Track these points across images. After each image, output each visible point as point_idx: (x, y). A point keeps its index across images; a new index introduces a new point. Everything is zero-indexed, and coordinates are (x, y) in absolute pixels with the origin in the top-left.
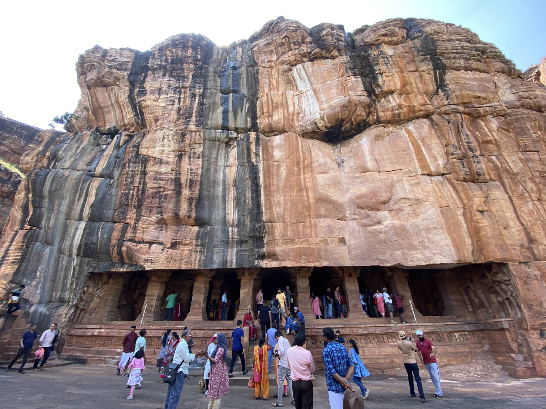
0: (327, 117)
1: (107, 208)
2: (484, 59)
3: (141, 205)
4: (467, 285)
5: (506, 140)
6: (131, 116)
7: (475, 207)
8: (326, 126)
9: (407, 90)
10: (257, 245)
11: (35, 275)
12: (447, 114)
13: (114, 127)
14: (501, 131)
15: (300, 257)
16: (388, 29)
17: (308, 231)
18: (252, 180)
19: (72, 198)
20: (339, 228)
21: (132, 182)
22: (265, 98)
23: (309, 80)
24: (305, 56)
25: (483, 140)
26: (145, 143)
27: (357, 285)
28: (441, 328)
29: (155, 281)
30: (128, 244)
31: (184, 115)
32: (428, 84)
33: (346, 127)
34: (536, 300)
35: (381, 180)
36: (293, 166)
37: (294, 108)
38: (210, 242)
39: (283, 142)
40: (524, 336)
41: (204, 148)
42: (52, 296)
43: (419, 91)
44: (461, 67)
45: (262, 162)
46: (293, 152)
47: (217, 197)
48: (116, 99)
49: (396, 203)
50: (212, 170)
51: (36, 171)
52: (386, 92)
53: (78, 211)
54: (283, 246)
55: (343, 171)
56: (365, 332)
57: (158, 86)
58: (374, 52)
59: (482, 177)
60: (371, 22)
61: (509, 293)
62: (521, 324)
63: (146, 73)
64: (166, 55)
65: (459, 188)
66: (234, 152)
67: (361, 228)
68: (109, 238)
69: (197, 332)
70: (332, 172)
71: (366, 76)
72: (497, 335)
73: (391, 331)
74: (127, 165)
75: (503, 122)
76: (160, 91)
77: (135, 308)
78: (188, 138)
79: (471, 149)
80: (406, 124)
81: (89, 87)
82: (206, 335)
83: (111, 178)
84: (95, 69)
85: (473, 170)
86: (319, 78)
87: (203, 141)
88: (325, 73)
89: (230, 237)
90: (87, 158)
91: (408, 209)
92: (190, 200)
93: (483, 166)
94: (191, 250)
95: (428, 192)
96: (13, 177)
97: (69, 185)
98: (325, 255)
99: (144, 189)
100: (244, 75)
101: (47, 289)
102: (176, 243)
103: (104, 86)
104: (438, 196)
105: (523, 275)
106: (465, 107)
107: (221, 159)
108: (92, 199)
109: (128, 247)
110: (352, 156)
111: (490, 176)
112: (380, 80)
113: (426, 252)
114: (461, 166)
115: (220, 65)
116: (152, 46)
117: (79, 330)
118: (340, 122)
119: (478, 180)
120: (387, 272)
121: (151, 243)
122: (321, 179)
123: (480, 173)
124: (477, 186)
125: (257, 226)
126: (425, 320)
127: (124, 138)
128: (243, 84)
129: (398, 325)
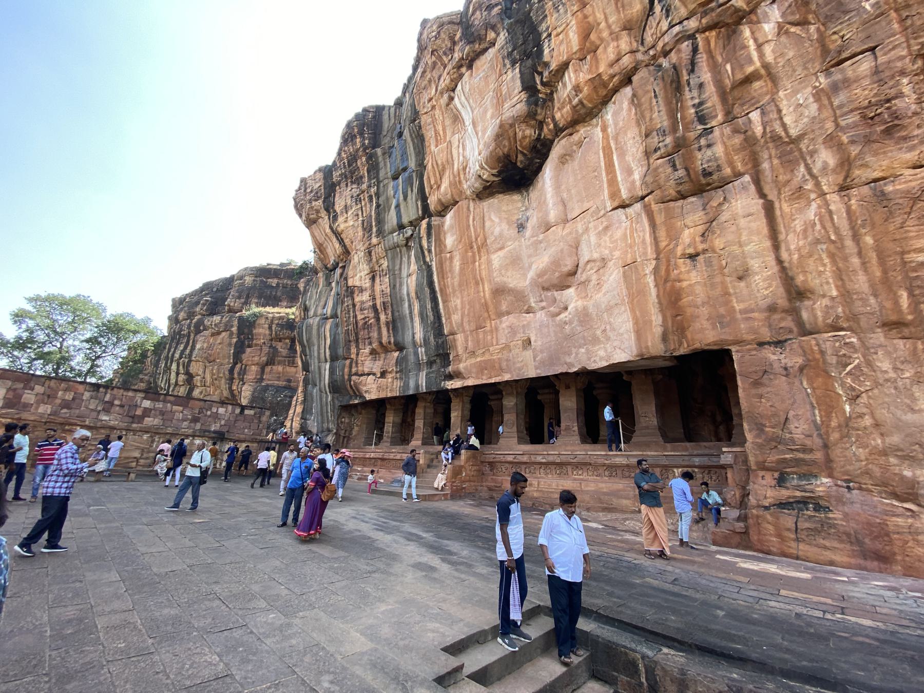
20: (524, 326)
22: (430, 164)
24: (461, 66)
30: (354, 378)
31: (367, 229)
33: (521, 162)
36: (466, 251)
50: (398, 285)
52: (557, 71)
56: (544, 461)
59: (715, 177)
65: (659, 219)
68: (343, 375)
76: (346, 208)
79: (702, 119)
85: (694, 169)
92: (387, 324)
106: (705, 13)
111: (733, 168)
112: (546, 51)
114: (670, 170)
119: (709, 184)
121: (368, 374)
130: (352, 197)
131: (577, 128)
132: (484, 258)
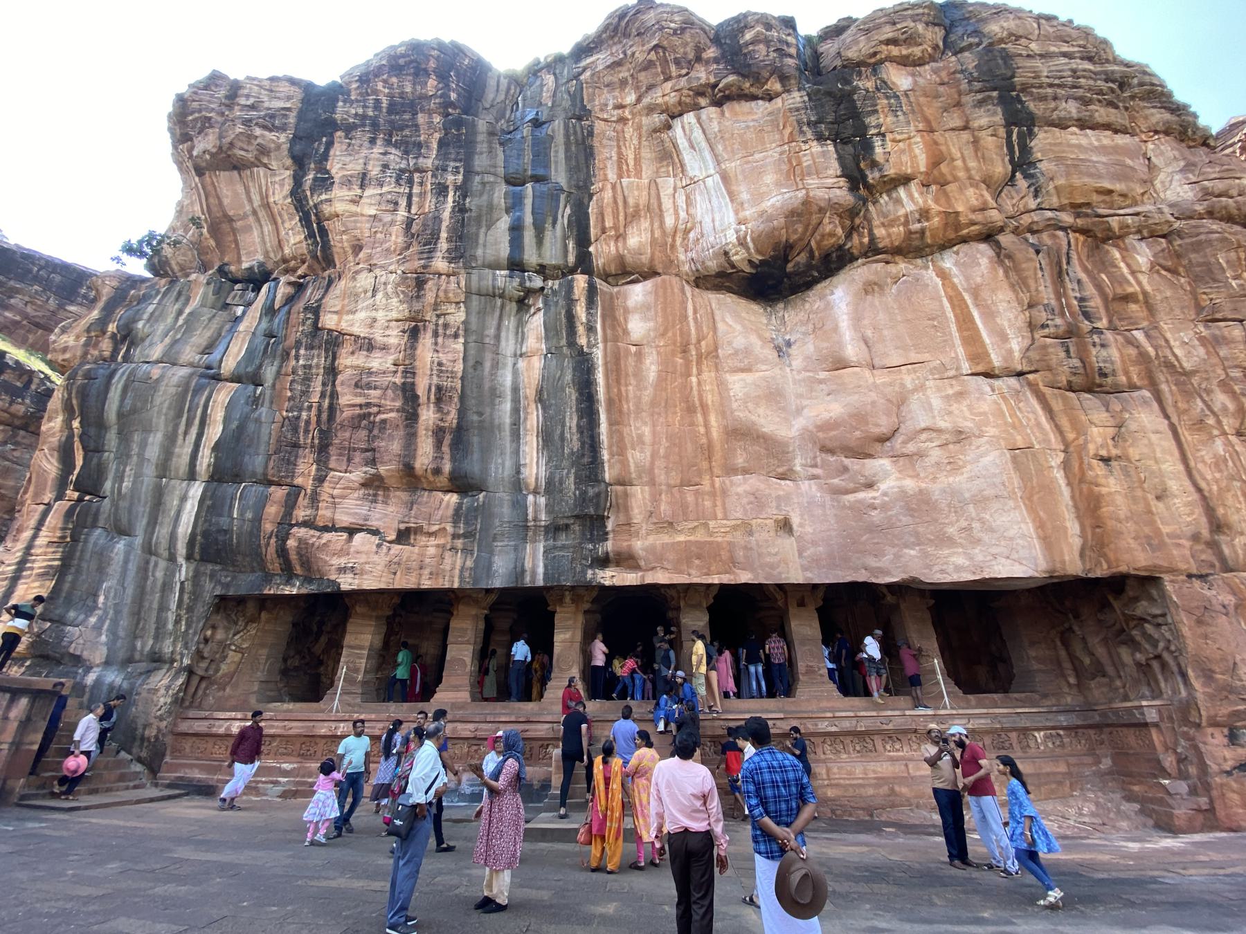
0: (753, 240)
1: (251, 450)
2: (1124, 101)
3: (327, 446)
4: (1066, 625)
5: (1168, 294)
6: (298, 240)
7: (1092, 448)
8: (750, 261)
9: (942, 174)
10: (592, 534)
11: (95, 602)
12: (1033, 232)
13: (261, 265)
14: (1158, 272)
15: (689, 561)
16: (899, 26)
17: (708, 504)
18: (579, 388)
19: (170, 429)
20: (778, 497)
21: (306, 393)
23: (712, 150)
24: (702, 94)
25: (1115, 295)
26: (331, 302)
27: (816, 624)
28: (1004, 720)
29: (363, 616)
30: (302, 532)
31: (421, 236)
32: (992, 160)
33: (798, 263)
34: (1224, 659)
35: (875, 386)
36: (673, 354)
37: (677, 218)
38: (486, 529)
39: (651, 299)
40: (1193, 739)
41: (467, 313)
42: (134, 648)
43: (970, 178)
44: (1071, 119)
45: (601, 345)
46: (674, 321)
47: (500, 427)
48: (262, 199)
49: (910, 439)
50: (487, 365)
51: (87, 367)
52: (892, 180)
53: (186, 459)
54: (651, 539)
55: (790, 365)
56: (834, 729)
57: (359, 168)
58: (866, 83)
59: (1109, 380)
60: (861, 11)
61: (1161, 645)
62: (1185, 713)
63: (332, 135)
64: (376, 92)
65: (1057, 405)
66: (536, 322)
67: (828, 498)
68: (258, 520)
69: (460, 726)
70: (764, 367)
71: (845, 142)
72: (1131, 738)
73: (890, 727)
74: (293, 352)
75: (1163, 250)
76: (364, 180)
77: (318, 676)
78: (430, 289)
79: (1087, 315)
80: (937, 255)
81: (200, 172)
82: (479, 734)
83: (258, 384)
84: (211, 127)
85: (1090, 363)
86: (736, 146)
87: (466, 298)
88: (750, 135)
89: (530, 517)
90: (201, 337)
91: (936, 454)
92: (438, 433)
93: (1114, 353)
94: (443, 546)
95: (985, 414)
96: (36, 381)
97: (163, 398)
98: (746, 557)
99: (332, 409)
100: (560, 139)
101: (121, 633)
102: (408, 530)
103: (235, 168)
104: (1006, 423)
105: (1196, 604)
106: (1078, 215)
107: (507, 340)
108: (215, 432)
109: (300, 540)
110: (810, 330)
111: (1129, 378)
112: (878, 150)
113: (977, 551)
114: (1063, 355)
115: (503, 116)
116: (342, 73)
117: (197, 723)
118: (784, 251)
119: (1100, 386)
120: (885, 596)
121: (351, 531)
122: (738, 384)
123: (1107, 371)
124: (1097, 401)
125: (591, 492)
126: (968, 701)
127: (283, 290)
128: (556, 162)
129: (907, 713)
130: (385, 167)
131: (897, 258)
132: (708, 375)
